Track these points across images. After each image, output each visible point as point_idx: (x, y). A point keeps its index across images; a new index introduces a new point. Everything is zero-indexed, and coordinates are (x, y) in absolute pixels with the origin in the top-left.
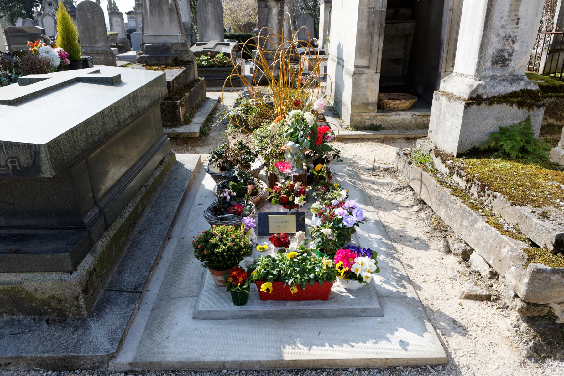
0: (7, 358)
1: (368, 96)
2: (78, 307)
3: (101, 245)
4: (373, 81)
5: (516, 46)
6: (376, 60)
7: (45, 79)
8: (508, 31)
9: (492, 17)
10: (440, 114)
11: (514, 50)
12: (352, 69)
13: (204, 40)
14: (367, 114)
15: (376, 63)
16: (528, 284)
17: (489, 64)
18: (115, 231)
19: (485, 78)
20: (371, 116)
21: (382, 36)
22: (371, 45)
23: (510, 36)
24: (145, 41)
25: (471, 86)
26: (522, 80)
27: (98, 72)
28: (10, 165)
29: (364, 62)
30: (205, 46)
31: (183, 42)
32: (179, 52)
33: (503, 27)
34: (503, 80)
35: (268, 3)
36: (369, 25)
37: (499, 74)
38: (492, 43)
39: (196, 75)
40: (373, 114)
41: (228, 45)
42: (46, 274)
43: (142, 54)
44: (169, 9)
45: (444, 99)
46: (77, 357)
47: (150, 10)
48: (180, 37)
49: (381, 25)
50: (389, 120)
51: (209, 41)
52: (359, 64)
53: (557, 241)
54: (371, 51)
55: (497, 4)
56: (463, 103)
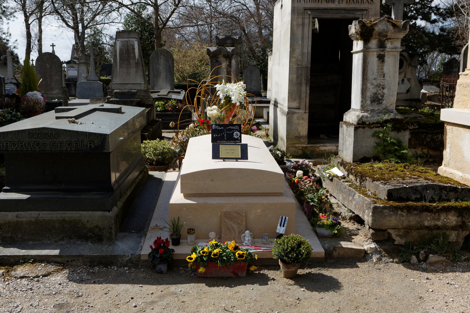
0: (73, 256)
1: (299, 131)
2: (111, 233)
3: (120, 204)
4: (303, 119)
5: (385, 91)
6: (305, 103)
7: (74, 109)
8: (378, 82)
9: (367, 73)
10: (343, 137)
11: (384, 94)
12: (286, 110)
13: (155, 88)
14: (299, 145)
15: (304, 105)
16: (372, 216)
17: (369, 102)
18: (124, 200)
19: (367, 111)
20: (303, 147)
21: (309, 85)
22: (301, 92)
23: (380, 85)
24: (113, 88)
25: (358, 116)
26: (392, 112)
27: (103, 106)
28: (88, 145)
29: (295, 104)
30: (159, 94)
31: (146, 89)
32: (142, 97)
33: (374, 79)
34: (379, 113)
35: (219, 59)
36: (298, 77)
37: (376, 109)
38: (369, 89)
39: (155, 116)
40: (305, 146)
41: (179, 93)
42: (94, 212)
43: (110, 98)
44: (135, 63)
45: (344, 126)
46: (115, 255)
47: (120, 63)
48: (143, 85)
49: (307, 77)
50: (318, 151)
51: (161, 89)
52: (291, 106)
53: (388, 193)
54: (300, 96)
55: (369, 65)
56: (353, 127)
